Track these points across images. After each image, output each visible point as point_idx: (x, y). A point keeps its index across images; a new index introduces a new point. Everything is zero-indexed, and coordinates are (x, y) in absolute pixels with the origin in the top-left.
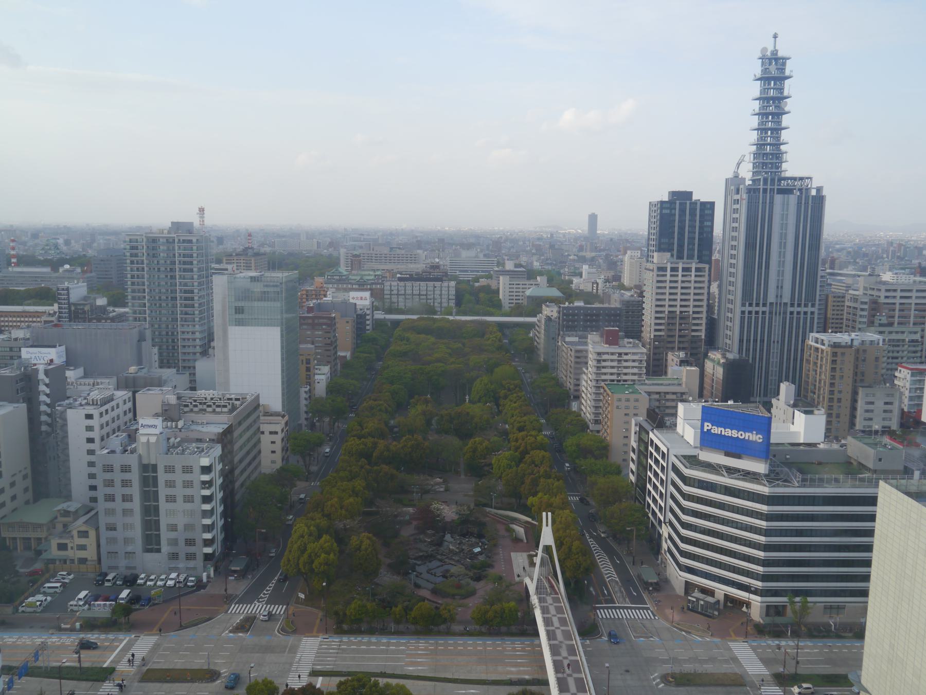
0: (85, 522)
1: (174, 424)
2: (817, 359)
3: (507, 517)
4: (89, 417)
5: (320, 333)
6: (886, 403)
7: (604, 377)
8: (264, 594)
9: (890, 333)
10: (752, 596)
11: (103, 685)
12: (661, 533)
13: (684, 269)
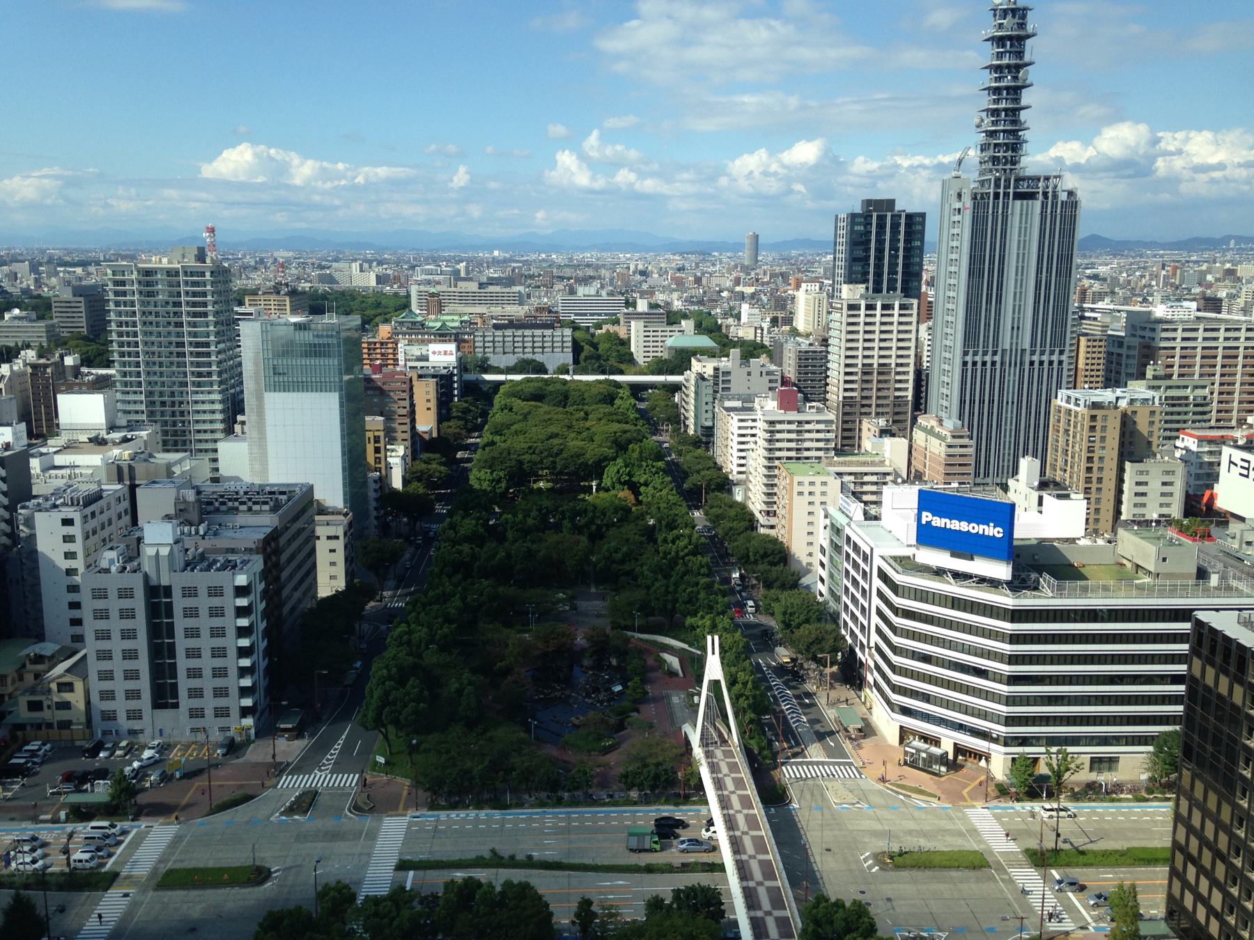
0: (68, 671)
1: (193, 528)
2: (1069, 425)
3: (655, 642)
4: (67, 522)
6: (1164, 484)
7: (778, 454)
8: (328, 760)
10: (993, 746)
11: (103, 897)
12: (864, 660)
13: (885, 307)
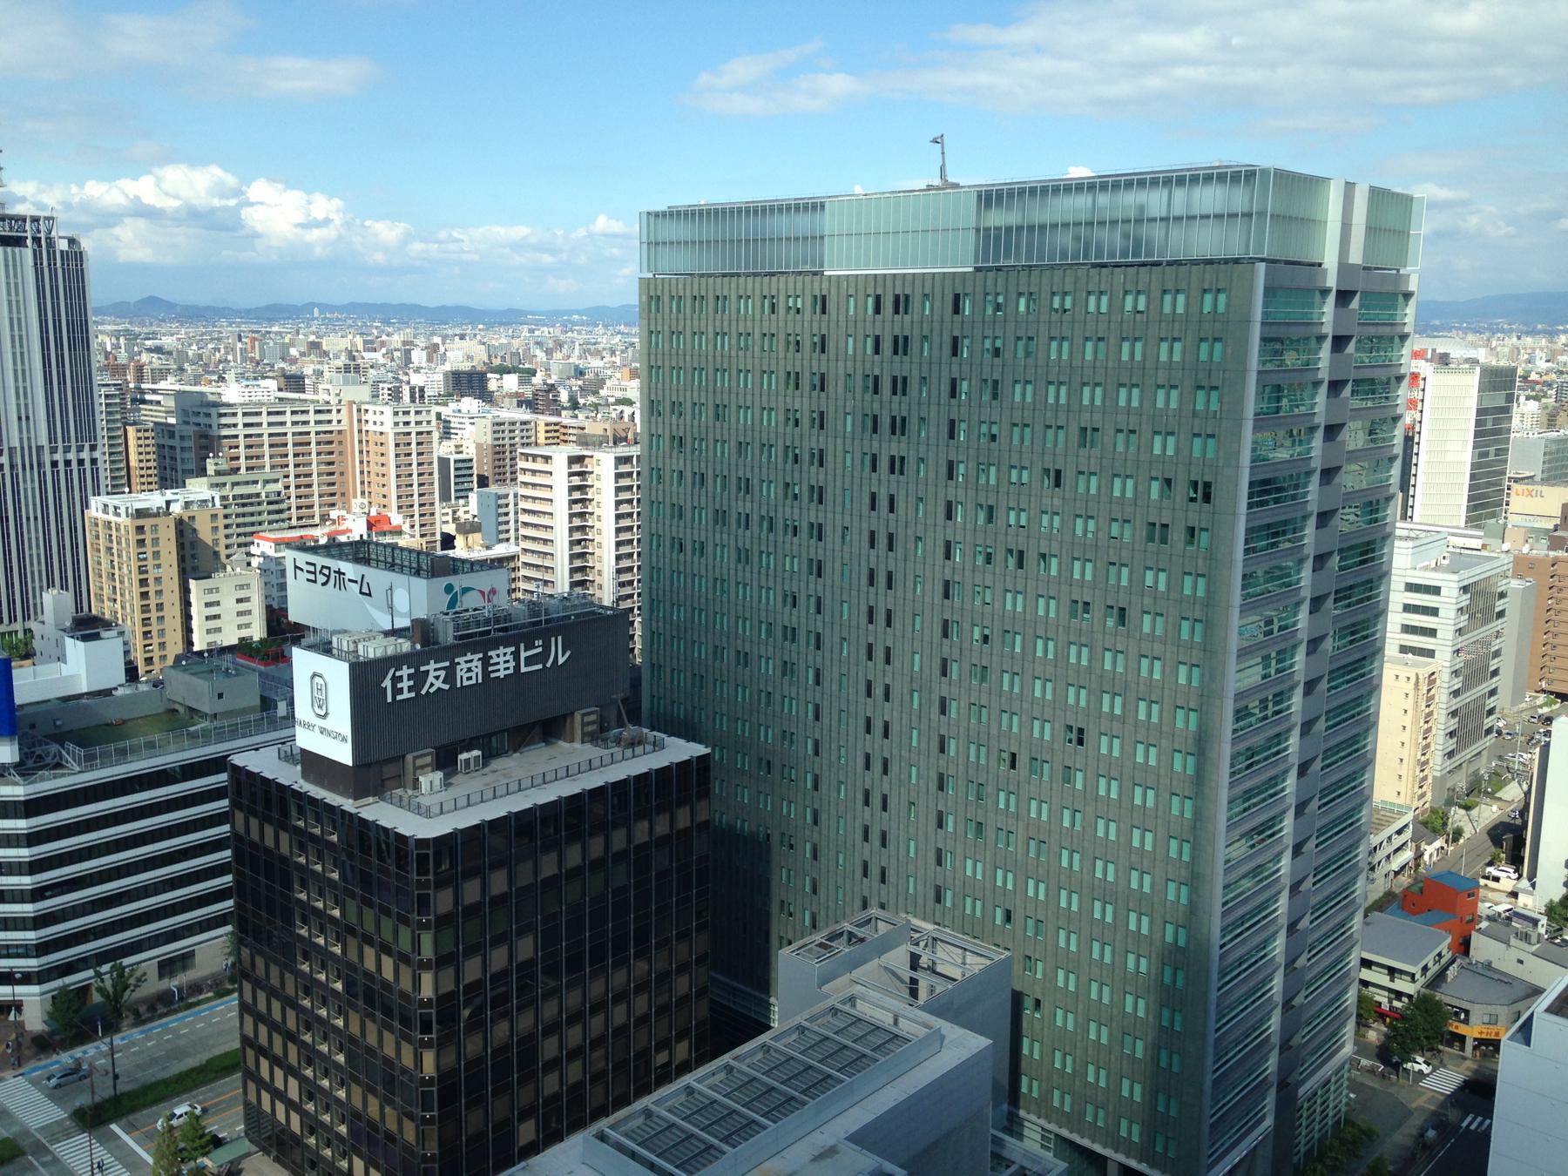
2: (111, 541)
6: (239, 601)
9: (234, 484)
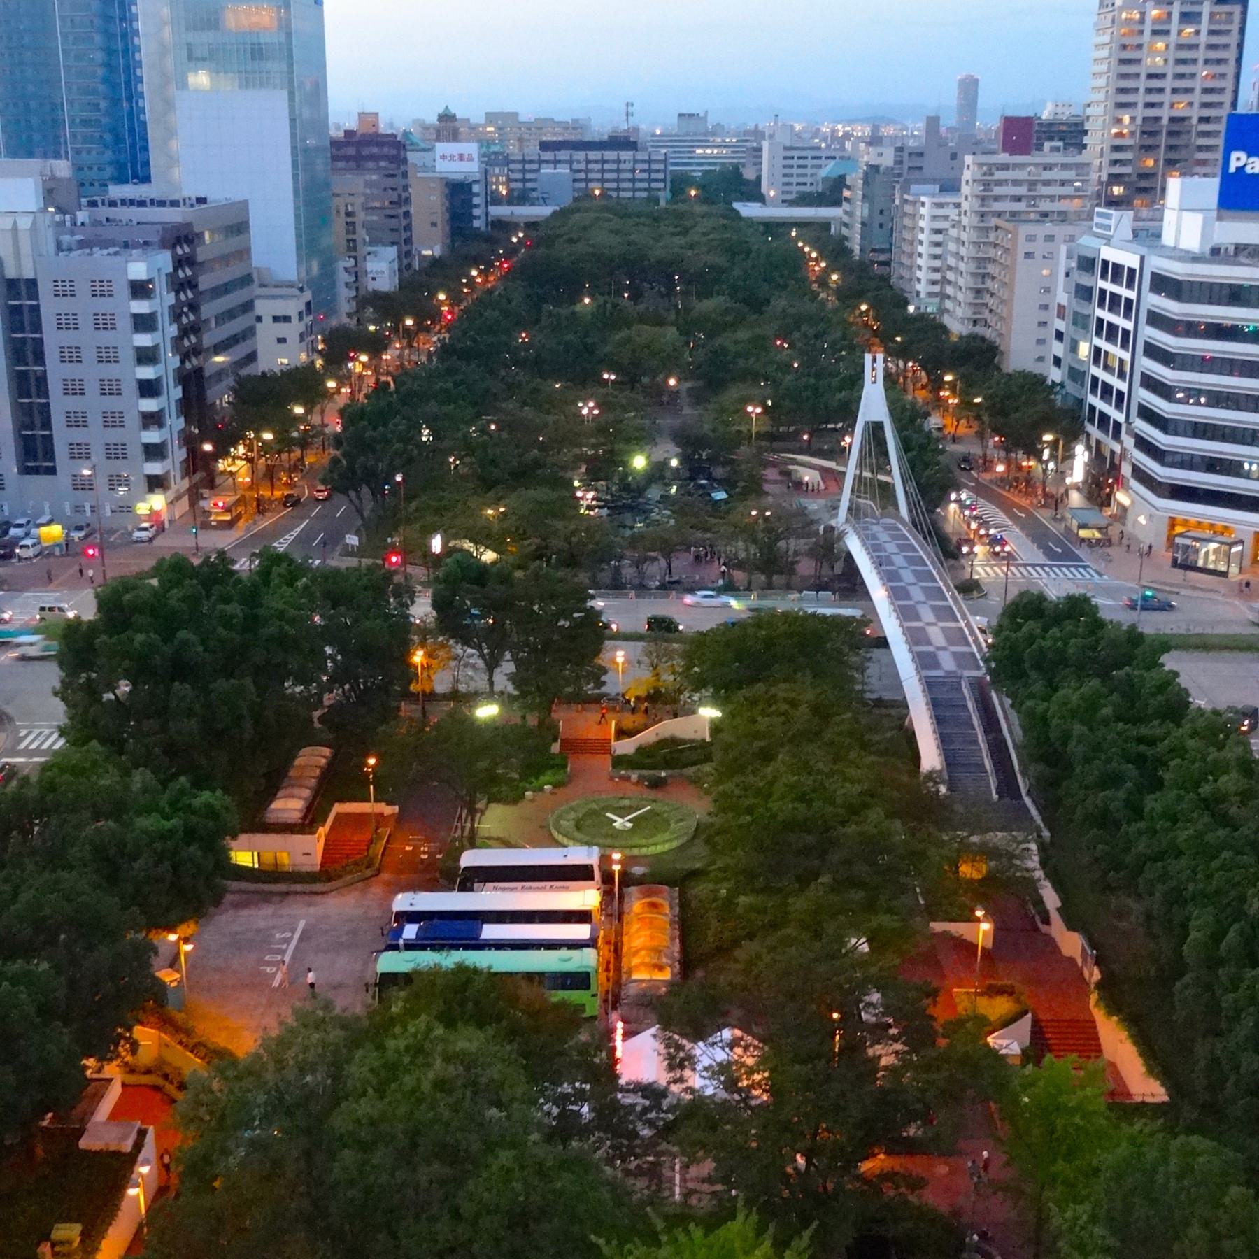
1: (68, 217)
5: (374, 177)
7: (997, 206)
